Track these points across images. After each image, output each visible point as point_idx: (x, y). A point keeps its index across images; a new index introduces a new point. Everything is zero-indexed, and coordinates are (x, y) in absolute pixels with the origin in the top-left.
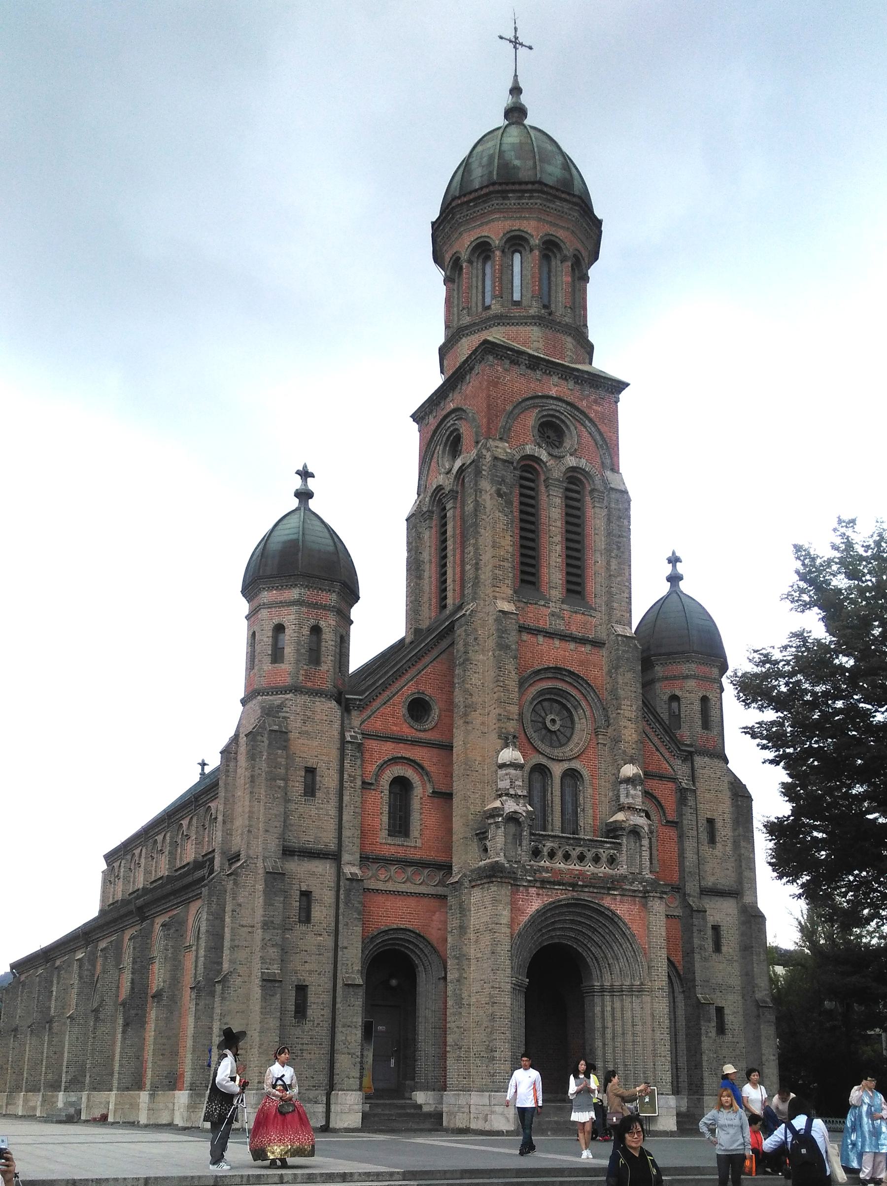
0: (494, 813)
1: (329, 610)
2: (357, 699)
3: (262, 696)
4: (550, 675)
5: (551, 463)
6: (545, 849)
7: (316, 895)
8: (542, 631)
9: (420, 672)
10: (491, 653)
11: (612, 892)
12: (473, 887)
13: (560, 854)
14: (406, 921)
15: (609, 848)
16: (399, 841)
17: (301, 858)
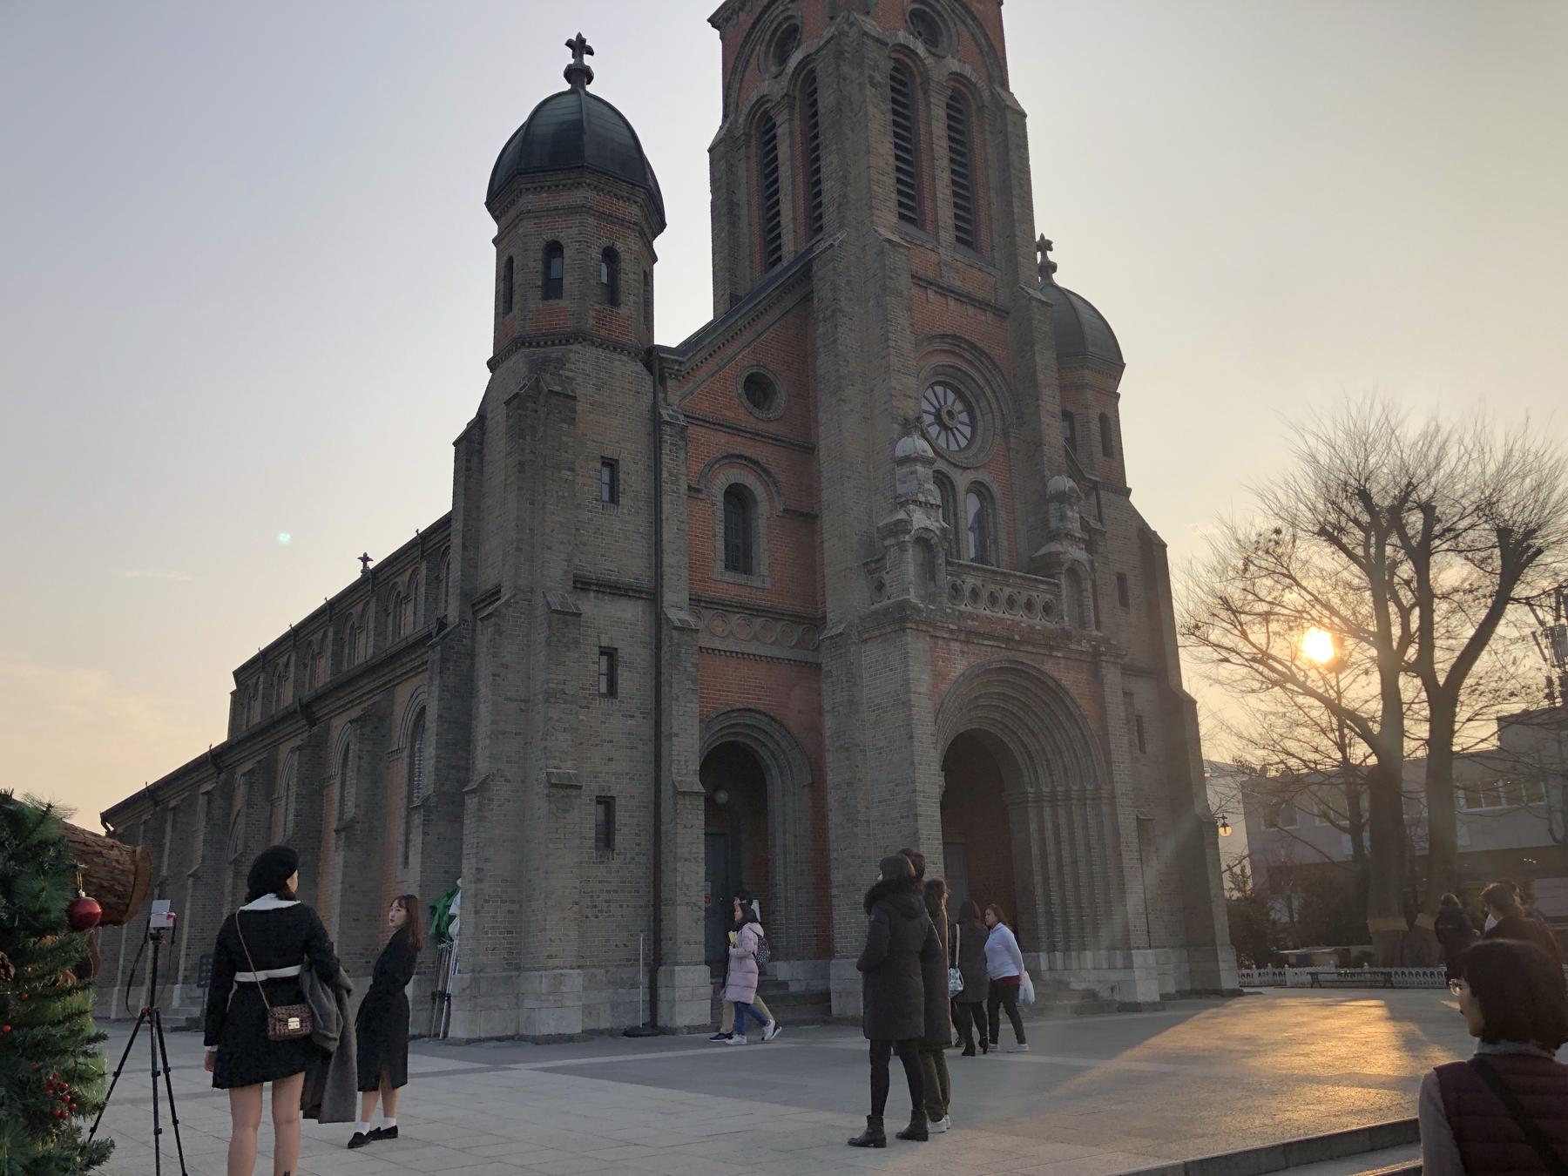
0: (900, 527)
1: (629, 228)
2: (677, 361)
3: (528, 347)
4: (946, 347)
5: (929, 61)
6: (964, 586)
7: (624, 652)
8: (931, 284)
9: (758, 337)
10: (872, 303)
11: (1055, 653)
12: (865, 641)
13: (985, 594)
14: (753, 699)
15: (1044, 591)
16: (741, 578)
17: (600, 595)
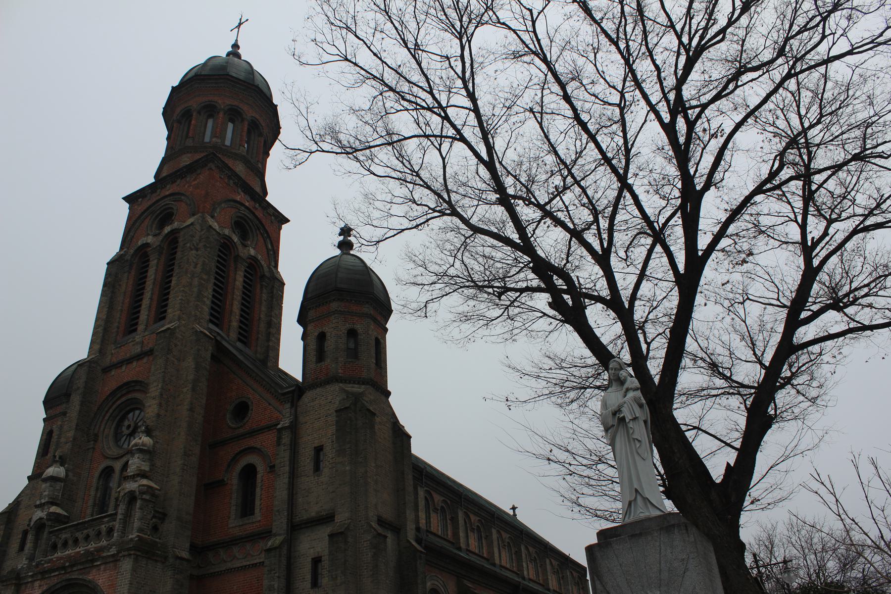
11: (95, 564)
